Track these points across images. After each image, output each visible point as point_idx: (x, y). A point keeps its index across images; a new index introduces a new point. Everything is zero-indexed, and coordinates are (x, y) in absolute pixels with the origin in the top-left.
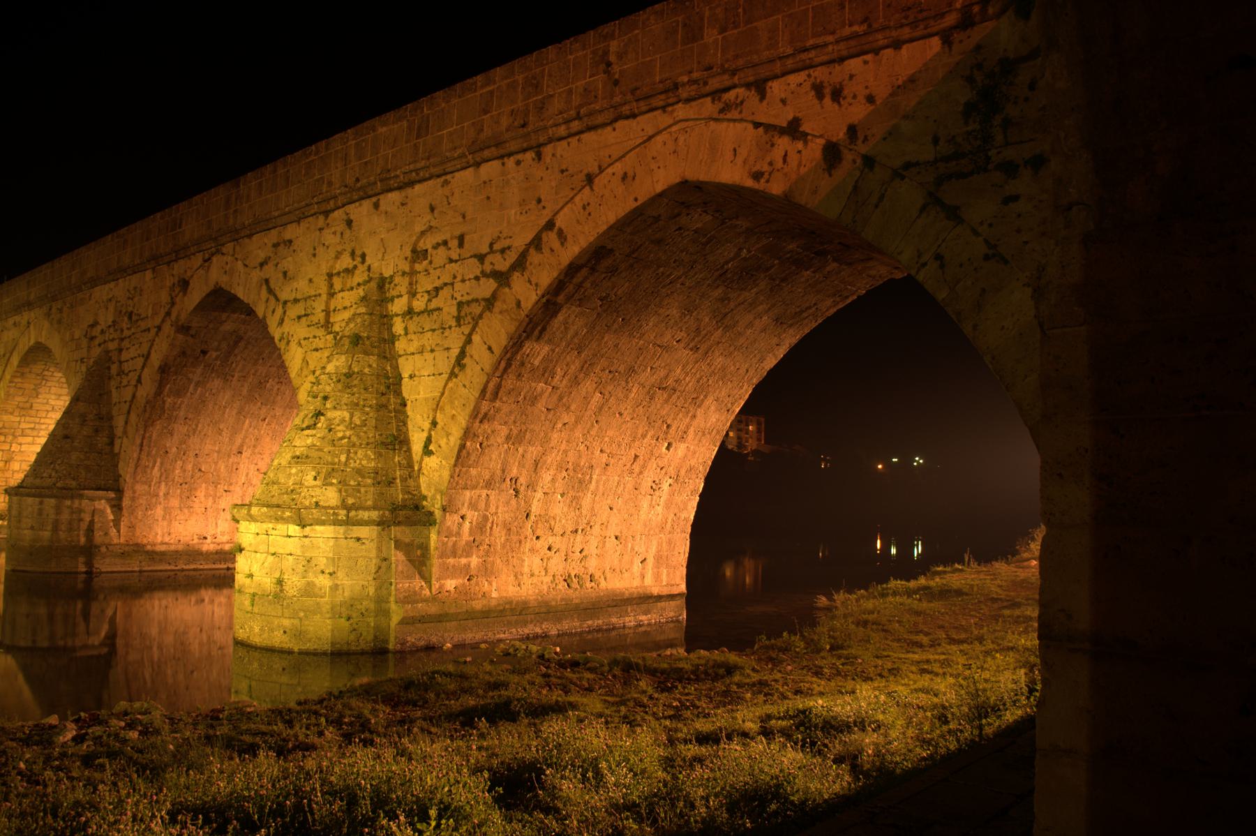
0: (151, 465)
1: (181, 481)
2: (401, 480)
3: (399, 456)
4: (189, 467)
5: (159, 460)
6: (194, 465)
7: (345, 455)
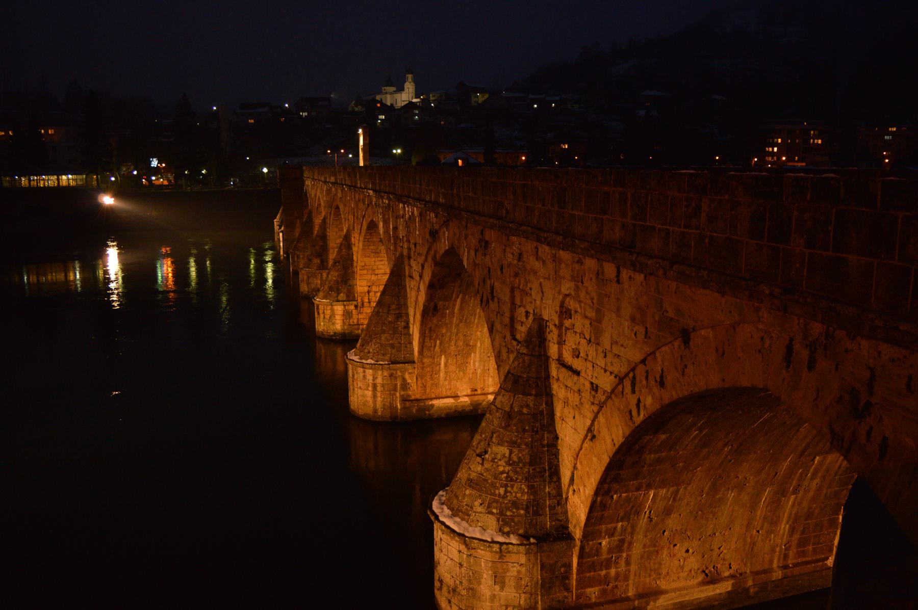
0: (433, 346)
1: (456, 354)
2: (549, 508)
3: (549, 488)
4: (461, 343)
5: (438, 342)
6: (464, 342)
7: (504, 488)
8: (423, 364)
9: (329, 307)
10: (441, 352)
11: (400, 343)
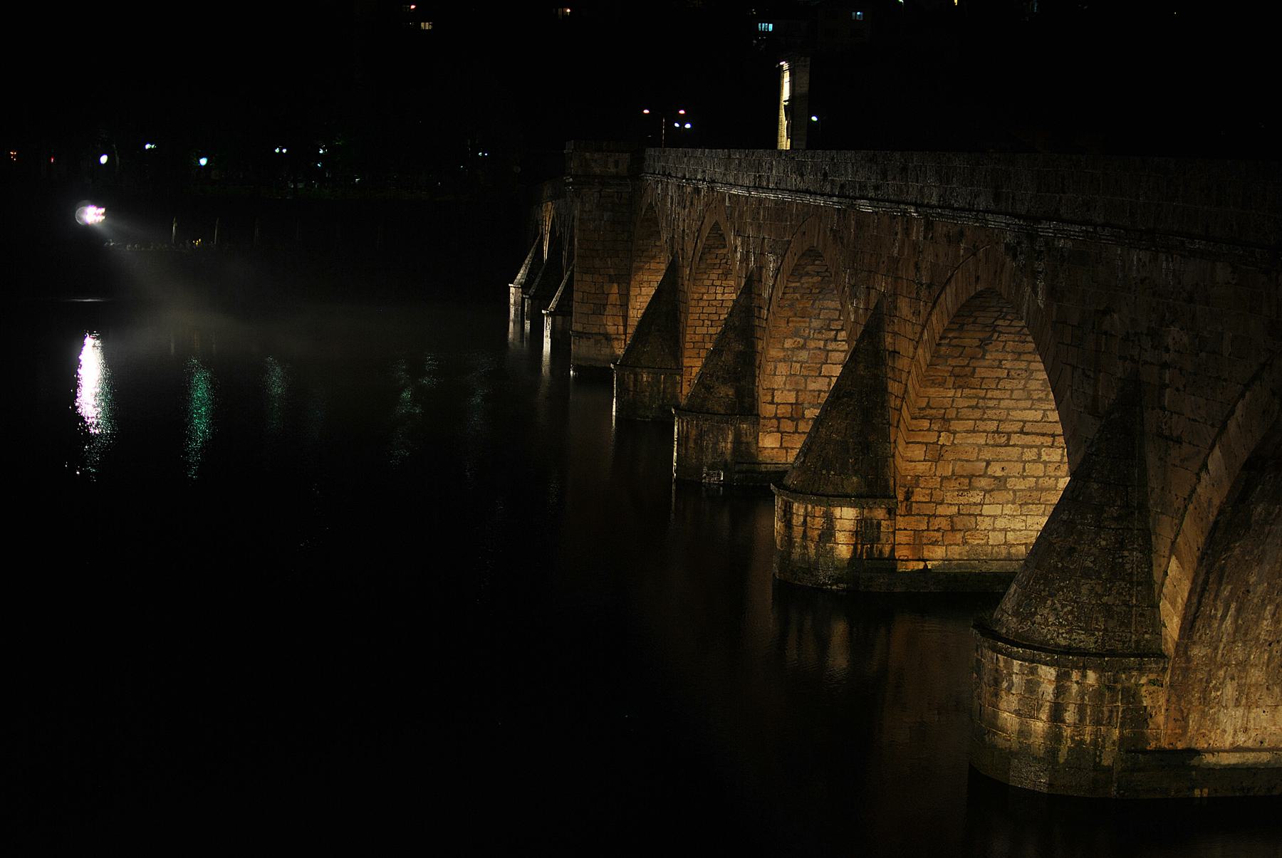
5: (1233, 606)
8: (1189, 660)
9: (819, 511)
10: (1237, 630)
11: (1125, 604)
